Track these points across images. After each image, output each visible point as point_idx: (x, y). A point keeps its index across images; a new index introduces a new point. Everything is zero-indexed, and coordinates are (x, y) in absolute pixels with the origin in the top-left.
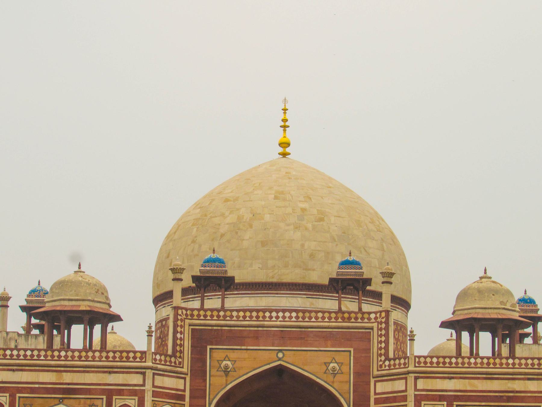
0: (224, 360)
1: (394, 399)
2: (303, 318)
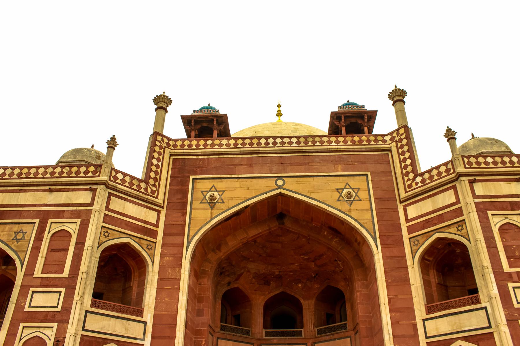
0: (210, 191)
1: (441, 219)
2: (306, 143)
